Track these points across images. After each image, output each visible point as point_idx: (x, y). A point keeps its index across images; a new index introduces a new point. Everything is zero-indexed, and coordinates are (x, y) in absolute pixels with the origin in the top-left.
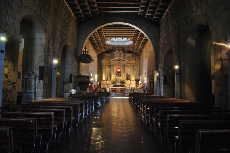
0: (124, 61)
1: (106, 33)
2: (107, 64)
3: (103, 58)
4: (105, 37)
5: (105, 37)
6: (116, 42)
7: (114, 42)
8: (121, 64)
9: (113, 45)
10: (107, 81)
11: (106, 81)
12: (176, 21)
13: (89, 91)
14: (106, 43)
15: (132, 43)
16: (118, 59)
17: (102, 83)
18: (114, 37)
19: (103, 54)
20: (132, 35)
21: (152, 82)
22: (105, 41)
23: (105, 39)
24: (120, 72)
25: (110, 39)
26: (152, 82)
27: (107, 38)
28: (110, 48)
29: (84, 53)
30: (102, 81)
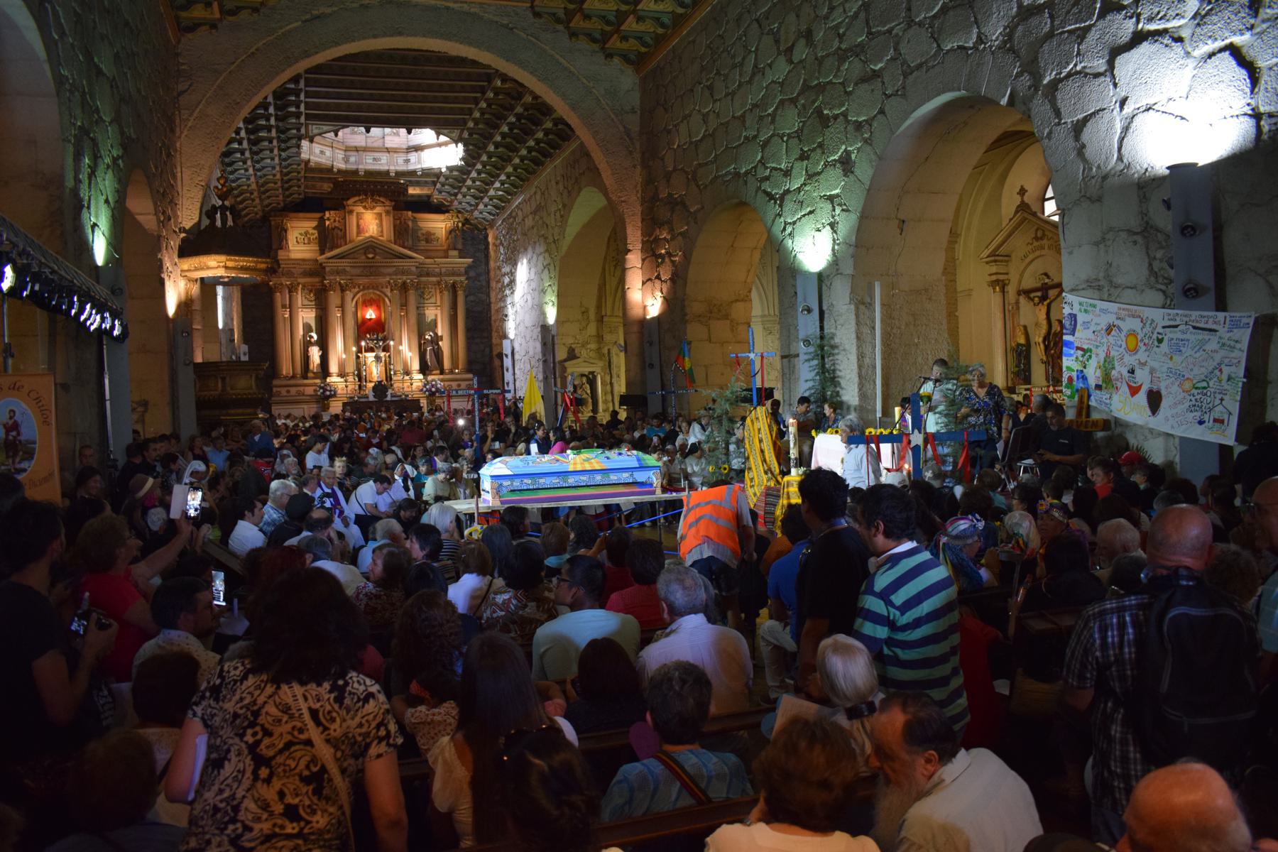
0: (398, 263)
1: (317, 95)
3: (274, 247)
4: (302, 119)
5: (302, 119)
6: (357, 149)
9: (343, 166)
10: (306, 381)
12: (790, 61)
14: (304, 156)
16: (367, 248)
17: (279, 394)
18: (356, 121)
20: (470, 112)
22: (299, 146)
23: (303, 131)
27: (314, 129)
28: (314, 187)
29: (213, 220)
30: (275, 382)
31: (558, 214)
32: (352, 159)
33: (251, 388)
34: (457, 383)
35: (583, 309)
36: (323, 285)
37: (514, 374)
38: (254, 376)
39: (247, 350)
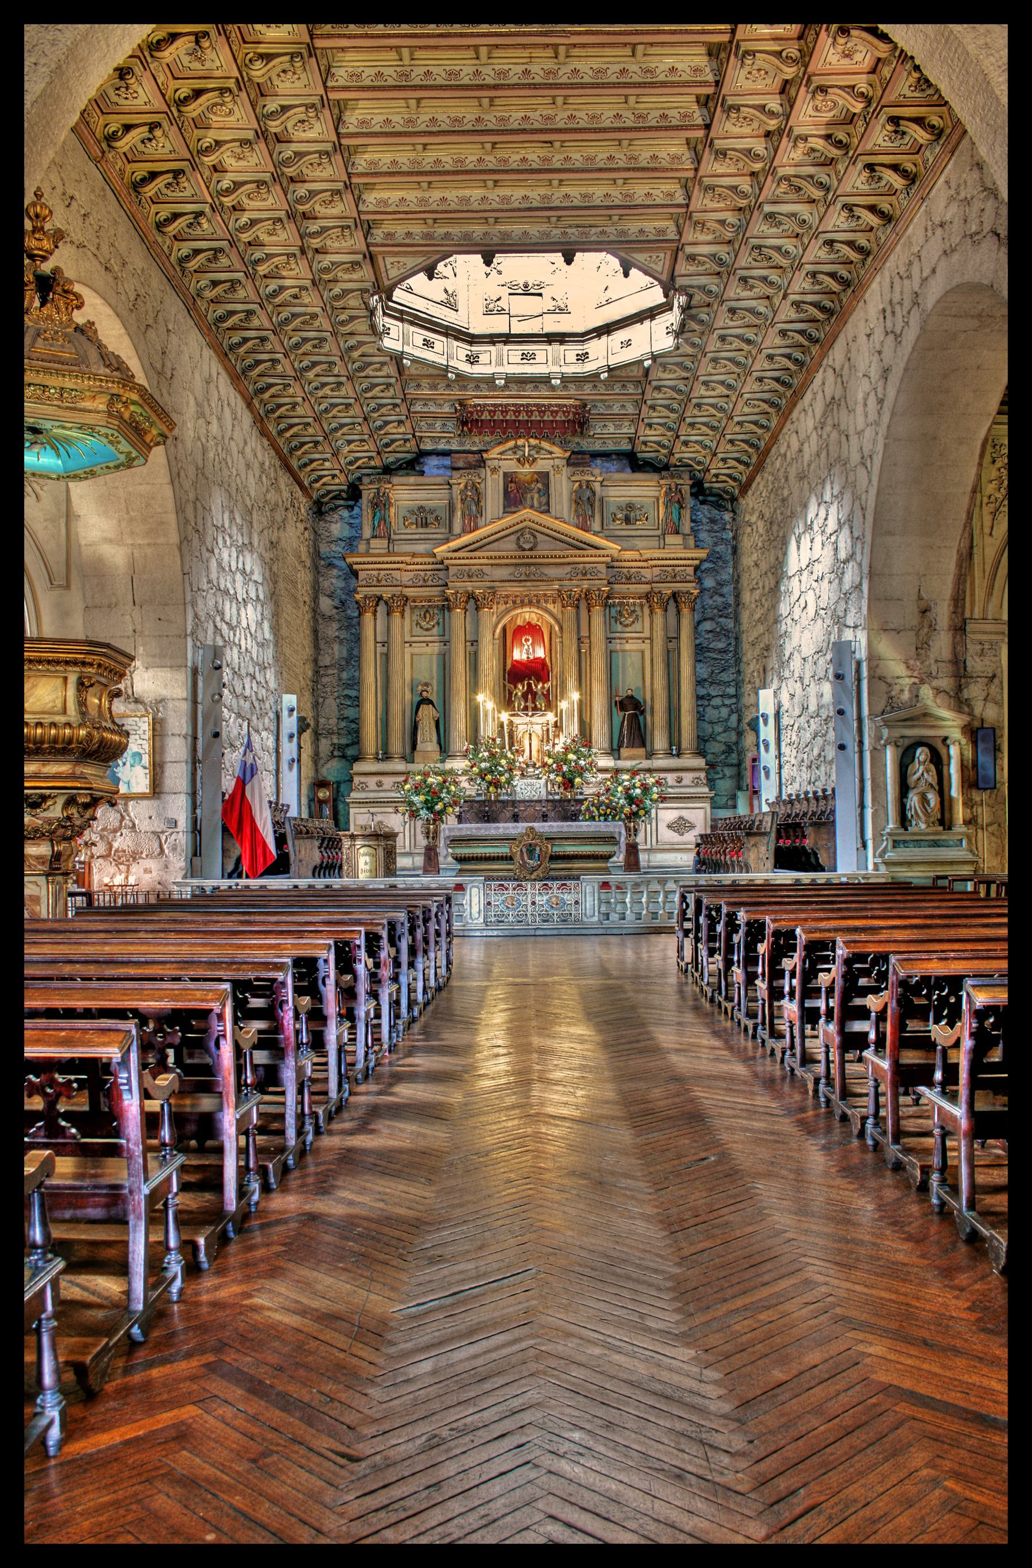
2: (410, 592)
6: (493, 339)
7: (472, 339)
8: (542, 589)
9: (466, 368)
11: (400, 766)
13: (193, 870)
15: (665, 343)
18: (467, 247)
19: (367, 494)
21: (922, 754)
24: (537, 670)
25: (422, 277)
26: (922, 754)
31: (872, 401)
32: (484, 358)
33: (64, 711)
34: (675, 775)
35: (923, 605)
36: (447, 600)
37: (779, 756)
38: (73, 679)
39: (294, 704)
